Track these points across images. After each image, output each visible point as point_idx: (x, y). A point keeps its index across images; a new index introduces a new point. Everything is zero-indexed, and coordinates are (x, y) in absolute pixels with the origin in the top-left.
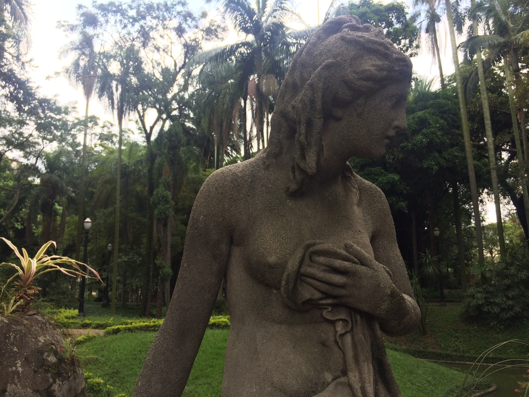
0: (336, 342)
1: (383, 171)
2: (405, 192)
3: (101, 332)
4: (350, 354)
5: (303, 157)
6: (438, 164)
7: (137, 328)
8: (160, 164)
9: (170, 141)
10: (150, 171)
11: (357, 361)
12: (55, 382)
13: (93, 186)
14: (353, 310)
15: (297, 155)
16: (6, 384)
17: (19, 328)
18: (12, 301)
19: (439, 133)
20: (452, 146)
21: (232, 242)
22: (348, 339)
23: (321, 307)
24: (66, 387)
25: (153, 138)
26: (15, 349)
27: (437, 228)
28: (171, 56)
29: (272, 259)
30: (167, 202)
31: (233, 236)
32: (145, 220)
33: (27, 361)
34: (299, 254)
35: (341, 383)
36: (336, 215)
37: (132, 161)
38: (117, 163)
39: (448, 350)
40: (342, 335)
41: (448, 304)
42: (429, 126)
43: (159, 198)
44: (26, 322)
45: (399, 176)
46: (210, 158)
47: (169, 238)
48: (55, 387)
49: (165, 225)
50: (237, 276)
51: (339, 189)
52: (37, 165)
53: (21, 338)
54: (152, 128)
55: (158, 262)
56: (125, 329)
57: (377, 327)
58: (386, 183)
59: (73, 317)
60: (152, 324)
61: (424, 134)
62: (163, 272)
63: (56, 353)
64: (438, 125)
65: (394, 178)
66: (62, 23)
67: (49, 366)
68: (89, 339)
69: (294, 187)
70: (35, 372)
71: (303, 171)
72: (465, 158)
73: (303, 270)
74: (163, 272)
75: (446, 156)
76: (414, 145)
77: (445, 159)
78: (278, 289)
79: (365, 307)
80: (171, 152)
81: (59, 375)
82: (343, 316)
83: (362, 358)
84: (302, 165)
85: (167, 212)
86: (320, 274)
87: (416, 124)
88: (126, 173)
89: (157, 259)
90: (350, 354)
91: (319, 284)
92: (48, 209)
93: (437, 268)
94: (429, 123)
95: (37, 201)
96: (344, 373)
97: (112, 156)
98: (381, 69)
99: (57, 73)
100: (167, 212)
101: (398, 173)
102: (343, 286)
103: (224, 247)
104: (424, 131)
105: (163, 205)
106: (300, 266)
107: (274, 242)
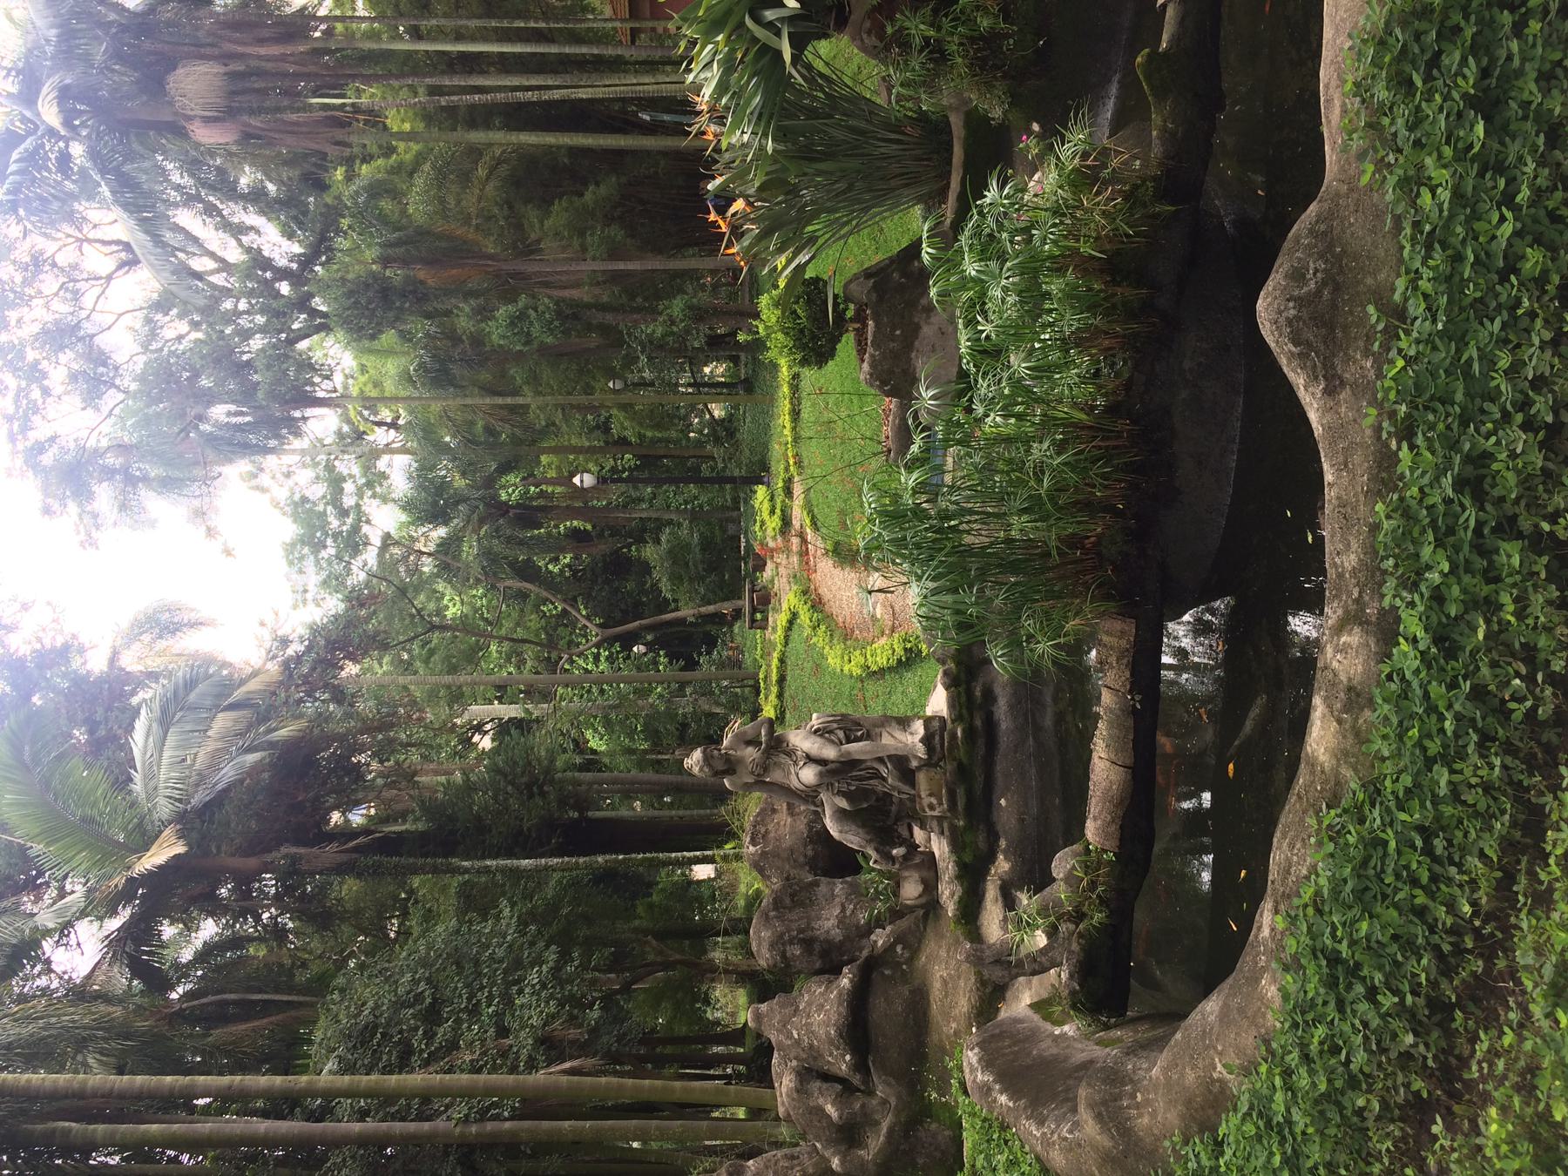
3: (798, 490)
7: (794, 429)
13: (472, 423)
28: (109, 278)
30: (522, 316)
36: (740, 761)
59: (772, 499)
66: (82, 537)
68: (809, 507)
88: (438, 373)
99: (210, 532)
105: (531, 323)
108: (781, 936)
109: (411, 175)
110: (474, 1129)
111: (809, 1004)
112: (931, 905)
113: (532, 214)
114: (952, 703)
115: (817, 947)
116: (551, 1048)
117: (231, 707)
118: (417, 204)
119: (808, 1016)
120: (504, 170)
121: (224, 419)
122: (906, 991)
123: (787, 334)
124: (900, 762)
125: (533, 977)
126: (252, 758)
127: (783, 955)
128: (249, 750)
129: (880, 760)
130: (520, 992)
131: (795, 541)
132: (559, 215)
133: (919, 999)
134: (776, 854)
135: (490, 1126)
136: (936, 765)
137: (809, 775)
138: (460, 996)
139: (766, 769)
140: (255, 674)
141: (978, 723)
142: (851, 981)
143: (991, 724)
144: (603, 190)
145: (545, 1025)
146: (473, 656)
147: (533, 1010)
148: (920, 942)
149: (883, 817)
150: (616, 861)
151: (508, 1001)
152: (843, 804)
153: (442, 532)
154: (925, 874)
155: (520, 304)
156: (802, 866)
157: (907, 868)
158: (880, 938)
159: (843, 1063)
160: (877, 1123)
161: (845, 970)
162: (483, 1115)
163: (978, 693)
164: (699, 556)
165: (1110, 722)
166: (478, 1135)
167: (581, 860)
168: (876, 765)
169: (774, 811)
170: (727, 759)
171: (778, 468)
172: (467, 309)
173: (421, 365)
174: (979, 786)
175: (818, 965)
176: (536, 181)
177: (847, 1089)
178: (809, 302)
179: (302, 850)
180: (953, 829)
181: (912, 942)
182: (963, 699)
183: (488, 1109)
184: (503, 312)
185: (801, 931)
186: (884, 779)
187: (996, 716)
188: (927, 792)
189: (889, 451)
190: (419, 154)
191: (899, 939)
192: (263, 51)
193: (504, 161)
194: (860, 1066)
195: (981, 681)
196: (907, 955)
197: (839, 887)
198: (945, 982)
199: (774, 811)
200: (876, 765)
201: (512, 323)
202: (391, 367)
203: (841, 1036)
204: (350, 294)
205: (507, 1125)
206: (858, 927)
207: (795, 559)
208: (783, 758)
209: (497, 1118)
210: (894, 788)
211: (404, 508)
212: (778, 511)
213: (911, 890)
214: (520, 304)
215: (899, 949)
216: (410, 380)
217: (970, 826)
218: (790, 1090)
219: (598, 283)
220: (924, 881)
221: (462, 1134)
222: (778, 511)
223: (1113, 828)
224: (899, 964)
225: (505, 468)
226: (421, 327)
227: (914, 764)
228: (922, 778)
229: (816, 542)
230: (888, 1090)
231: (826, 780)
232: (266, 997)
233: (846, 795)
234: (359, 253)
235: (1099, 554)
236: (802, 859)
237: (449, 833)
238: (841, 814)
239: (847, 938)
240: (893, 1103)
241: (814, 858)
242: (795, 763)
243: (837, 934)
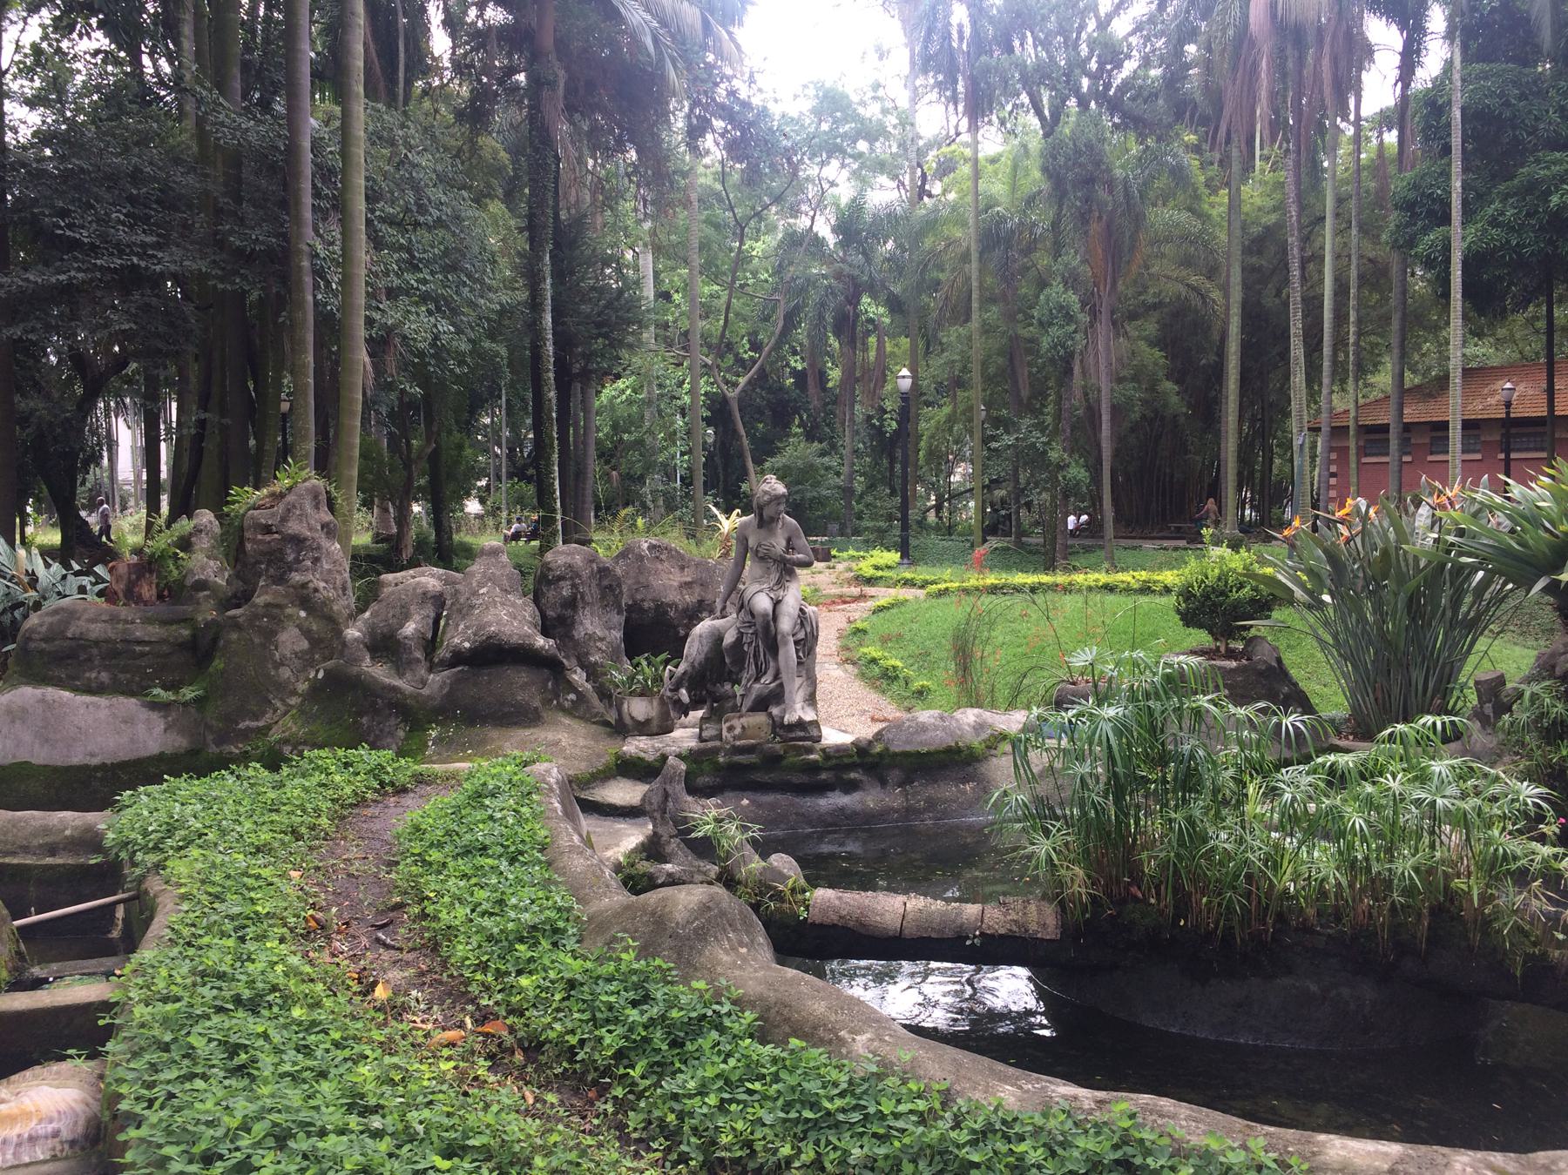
7: (977, 589)
10: (1055, 225)
30: (1070, 318)
36: (772, 532)
52: (815, 229)
56: (958, 589)
59: (889, 567)
88: (997, 238)
92: (848, 326)
95: (821, 317)
108: (579, 576)
109: (1189, 209)
110: (306, 264)
111: (513, 605)
112: (622, 729)
113: (1151, 327)
114: (840, 750)
115: (569, 612)
116: (378, 346)
117: (706, 25)
118: (1164, 216)
119: (503, 604)
120: (1196, 302)
121: (954, 20)
122: (536, 703)
123: (1219, 579)
124: (777, 696)
125: (445, 326)
126: (649, 41)
127: (561, 578)
128: (656, 40)
129: (777, 676)
130: (430, 313)
131: (855, 591)
132: (1154, 357)
133: (525, 717)
134: (640, 571)
135: (308, 280)
136: (776, 734)
137: (763, 603)
138: (425, 251)
139: (762, 559)
140: (738, 47)
141: (824, 776)
142: (542, 648)
143: (822, 789)
144: (1174, 399)
145: (405, 337)
146: (711, 271)
147: (419, 325)
148: (580, 718)
149: (711, 684)
150: (550, 411)
151: (425, 298)
152: (729, 638)
153: (831, 240)
154: (655, 723)
155: (1081, 316)
156: (632, 597)
157: (662, 702)
158: (578, 677)
159: (460, 637)
160: (401, 675)
161: (551, 642)
162: (319, 273)
163: (853, 775)
164: (809, 495)
165: (944, 914)
166: (300, 268)
167: (551, 375)
168: (771, 673)
169: (682, 568)
170: (774, 520)
171: (921, 573)
172: (1075, 263)
173: (1002, 220)
174: (758, 777)
175: (551, 613)
176: (1185, 335)
177: (430, 644)
178: (1252, 601)
179: (561, 92)
180: (715, 751)
181: (579, 709)
182: (846, 760)
183: (323, 278)
184: (1073, 299)
185: (583, 598)
186: (757, 680)
187: (830, 794)
188: (745, 726)
190: (1209, 217)
191: (581, 697)
192: (1326, 62)
193: (1204, 302)
194: (458, 658)
195: (864, 778)
196: (567, 704)
197: (618, 635)
198: (556, 744)
199: (682, 568)
200: (771, 673)
201: (1062, 307)
202: (996, 187)
203: (490, 637)
204: (1089, 146)
205: (310, 298)
206: (587, 654)
207: (835, 591)
208: (774, 576)
209: (316, 287)
210: (748, 690)
211: (854, 200)
212: (880, 573)
213: (639, 709)
214: (1081, 316)
215: (572, 696)
216: (988, 207)
217: (718, 768)
218: (425, 585)
219: (1086, 394)
220: (648, 721)
221: (300, 251)
222: (880, 573)
223: (835, 918)
224: (557, 697)
225: (895, 305)
226: (1041, 218)
227: (775, 711)
228: (760, 718)
229: (859, 611)
230: (436, 686)
231: (759, 621)
232: (402, 55)
234: (1124, 152)
235: (1123, 902)
236: (639, 597)
237: (558, 244)
238: (718, 638)
239: (577, 644)
240: (426, 691)
241: (642, 610)
242: (771, 589)
243: (579, 633)
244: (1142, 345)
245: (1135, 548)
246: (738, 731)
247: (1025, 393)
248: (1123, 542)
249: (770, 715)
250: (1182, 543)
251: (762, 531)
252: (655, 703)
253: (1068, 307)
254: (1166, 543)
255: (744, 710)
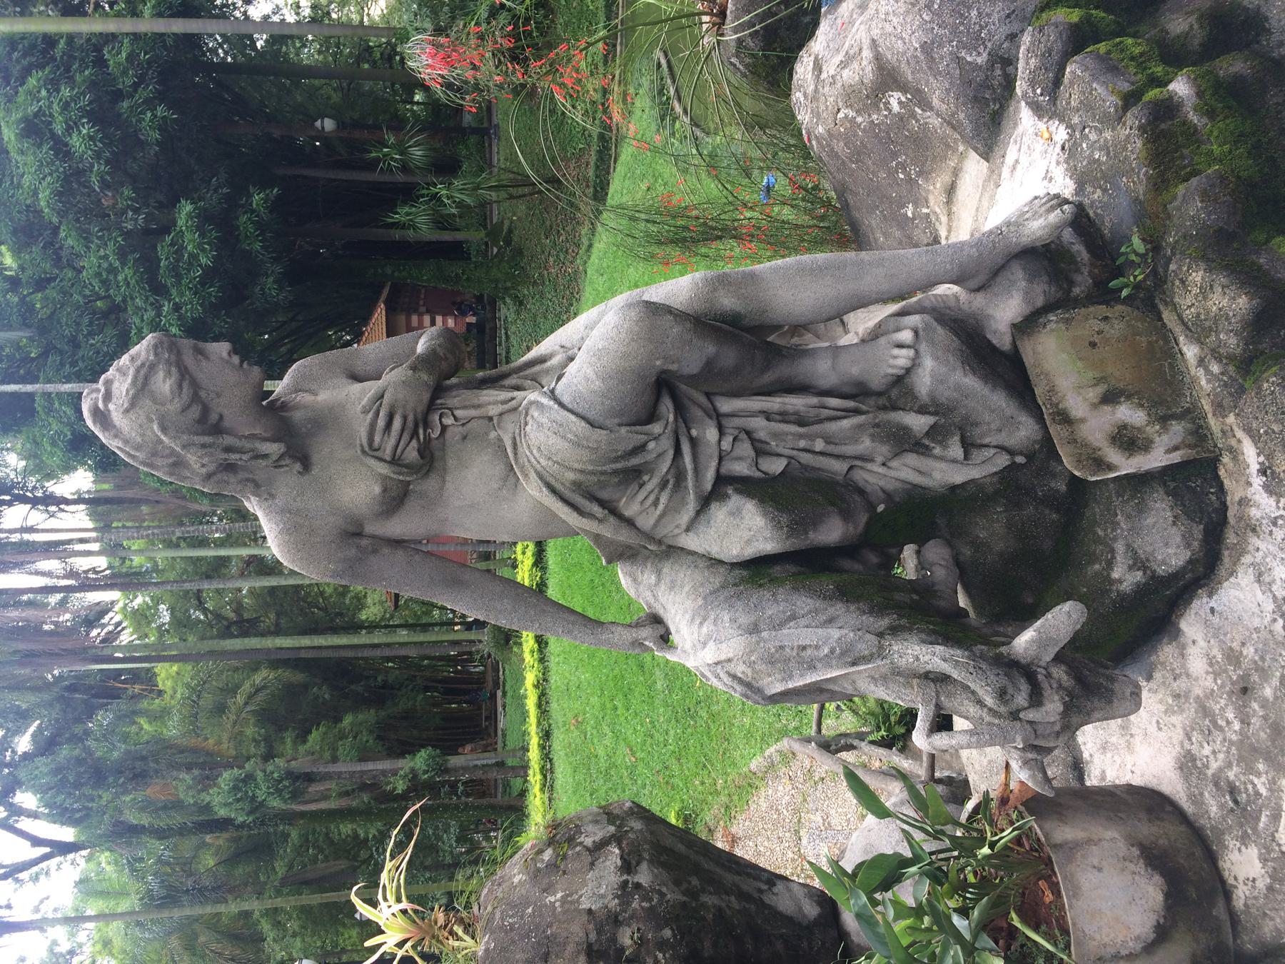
0: (463, 425)
1: (168, 239)
2: (225, 190)
4: (473, 413)
5: (265, 456)
6: (150, 104)
8: (142, 809)
9: (77, 785)
10: (161, 834)
11: (479, 406)
12: (581, 843)
14: (431, 406)
15: (263, 463)
16: (579, 911)
17: (498, 915)
18: (456, 944)
19: (66, 92)
20: (101, 62)
21: (359, 534)
22: (458, 413)
23: (428, 440)
24: (590, 828)
25: (67, 834)
26: (530, 910)
27: (318, 123)
29: (377, 489)
30: (250, 778)
31: (353, 532)
32: (294, 834)
33: (548, 890)
34: (372, 462)
35: (499, 423)
37: (134, 886)
38: (139, 924)
39: (590, 136)
40: (456, 419)
41: (495, 121)
42: (44, 115)
43: (238, 800)
44: (489, 908)
45: (183, 202)
46: (124, 682)
47: (339, 767)
48: (589, 842)
49: (309, 778)
50: (397, 527)
51: (297, 416)
53: (513, 907)
54: (36, 841)
55: (401, 786)
57: (448, 382)
58: (202, 235)
60: (539, 777)
61: (69, 130)
62: (425, 772)
63: (541, 852)
64: (44, 93)
65: (189, 216)
67: (558, 855)
69: (298, 466)
70: (564, 873)
71: (281, 457)
72: (136, 37)
73: (388, 459)
74: (425, 772)
75: (129, 82)
76: (98, 155)
77: (136, 86)
78: (409, 483)
79: (426, 397)
80: (111, 780)
81: (571, 840)
82: (437, 417)
83: (476, 402)
84: (275, 457)
85: (276, 775)
86: (392, 442)
87: (40, 146)
89: (395, 789)
90: (473, 413)
91: (402, 442)
93: (412, 137)
94: (36, 115)
96: (491, 419)
97: (118, 942)
98: (169, 373)
100: (276, 775)
101: (173, 202)
102: (405, 418)
103: (364, 542)
104: (59, 128)
105: (257, 786)
106: (385, 461)
107: (358, 487)
120: (260, 697)
144: (361, 717)
152: (744, 530)
154: (1147, 830)
189: (722, 14)
220: (1155, 858)
227: (1004, 311)
228: (1057, 360)
233: (761, 489)
244: (302, 749)
245: (504, 735)
246: (1130, 414)
247: (343, 864)
248: (500, 744)
249: (1027, 325)
250: (499, 693)
251: (325, 450)
252: (1065, 832)
253: (237, 779)
254: (500, 709)
255: (1025, 431)
